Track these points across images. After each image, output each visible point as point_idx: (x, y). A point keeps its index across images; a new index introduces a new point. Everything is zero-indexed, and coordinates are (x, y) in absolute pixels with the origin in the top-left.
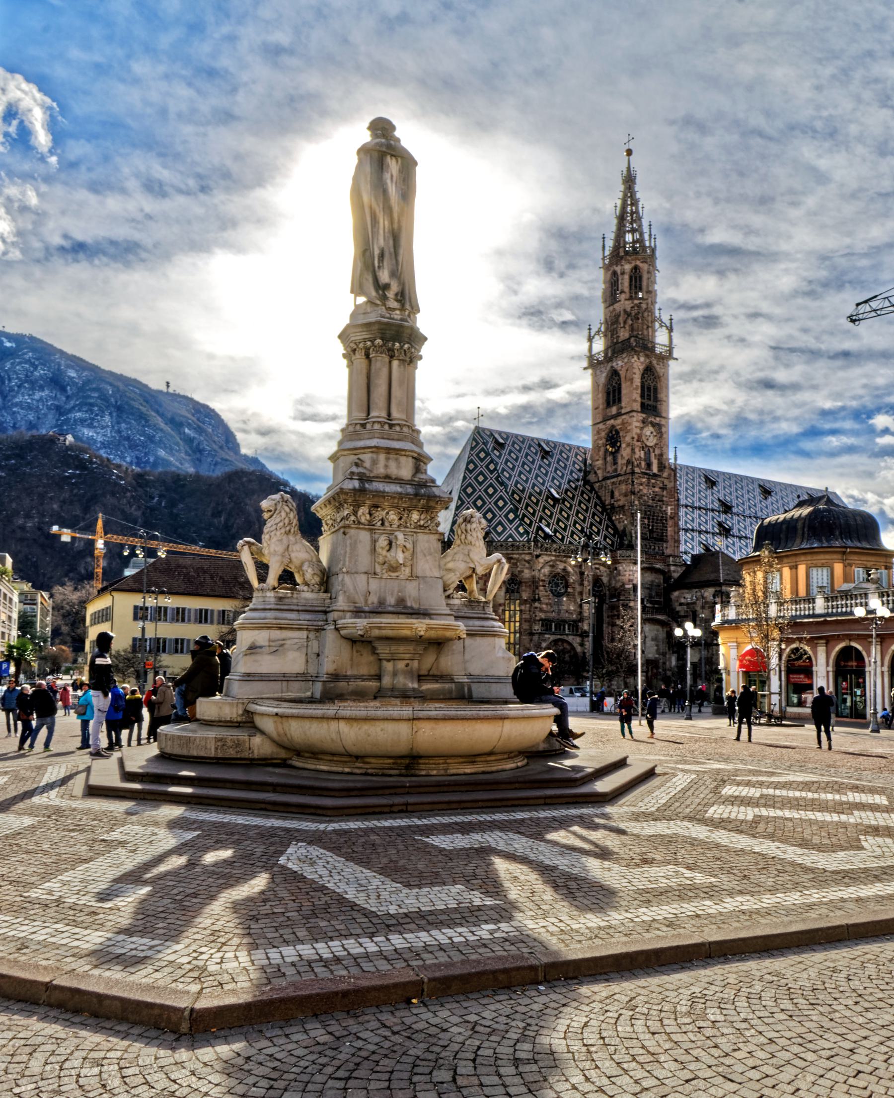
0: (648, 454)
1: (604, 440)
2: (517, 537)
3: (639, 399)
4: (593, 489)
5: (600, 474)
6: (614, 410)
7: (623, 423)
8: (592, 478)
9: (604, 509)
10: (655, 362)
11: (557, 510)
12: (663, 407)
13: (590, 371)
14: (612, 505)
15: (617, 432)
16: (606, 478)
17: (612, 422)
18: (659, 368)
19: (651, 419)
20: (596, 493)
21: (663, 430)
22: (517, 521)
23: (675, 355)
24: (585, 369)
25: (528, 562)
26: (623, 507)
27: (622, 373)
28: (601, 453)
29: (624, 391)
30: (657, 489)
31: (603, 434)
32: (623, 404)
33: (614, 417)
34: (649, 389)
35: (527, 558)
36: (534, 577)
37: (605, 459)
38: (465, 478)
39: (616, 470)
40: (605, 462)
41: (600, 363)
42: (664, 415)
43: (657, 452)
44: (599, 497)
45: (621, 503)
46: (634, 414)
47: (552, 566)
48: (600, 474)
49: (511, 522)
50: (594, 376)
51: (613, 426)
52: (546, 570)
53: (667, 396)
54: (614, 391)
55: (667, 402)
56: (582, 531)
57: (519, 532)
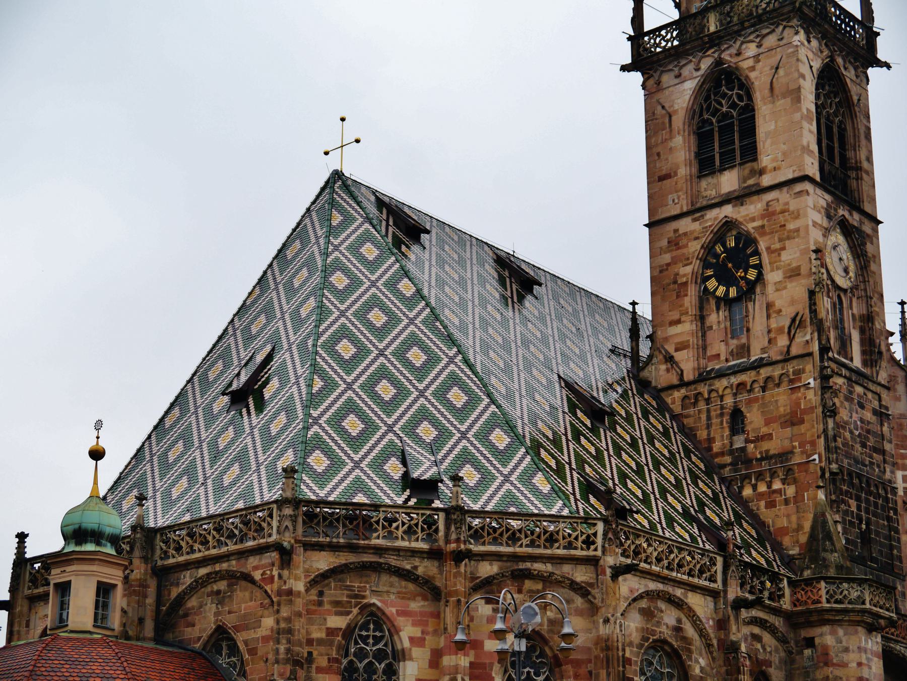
0: (838, 306)
1: (696, 265)
2: (534, 506)
3: (815, 148)
4: (663, 408)
5: (688, 363)
6: (729, 181)
7: (768, 213)
8: (659, 374)
9: (711, 469)
10: (840, 61)
11: (605, 440)
12: (865, 188)
13: (637, 77)
14: (741, 458)
15: (747, 242)
16: (704, 377)
17: (728, 210)
18: (849, 74)
19: (842, 212)
20: (674, 417)
21: (869, 247)
22: (521, 459)
23: (881, 55)
24: (624, 68)
25: (582, 590)
26: (784, 456)
27: (759, 79)
28: (690, 300)
29: (765, 126)
30: (868, 415)
31: (695, 247)
32: (765, 160)
33: (738, 198)
34: (829, 129)
35: (581, 575)
36: (606, 645)
37: (702, 318)
38: (322, 311)
39: (744, 350)
40: (704, 330)
41: (673, 55)
42: (867, 208)
43: (857, 308)
44: (688, 433)
45: (773, 446)
46: (807, 186)
47: (647, 614)
48: (688, 363)
49: (504, 456)
50: (651, 91)
51: (728, 225)
52: (634, 624)
53: (869, 159)
54: (726, 130)
55: (870, 173)
56: (686, 514)
57: (536, 491)
